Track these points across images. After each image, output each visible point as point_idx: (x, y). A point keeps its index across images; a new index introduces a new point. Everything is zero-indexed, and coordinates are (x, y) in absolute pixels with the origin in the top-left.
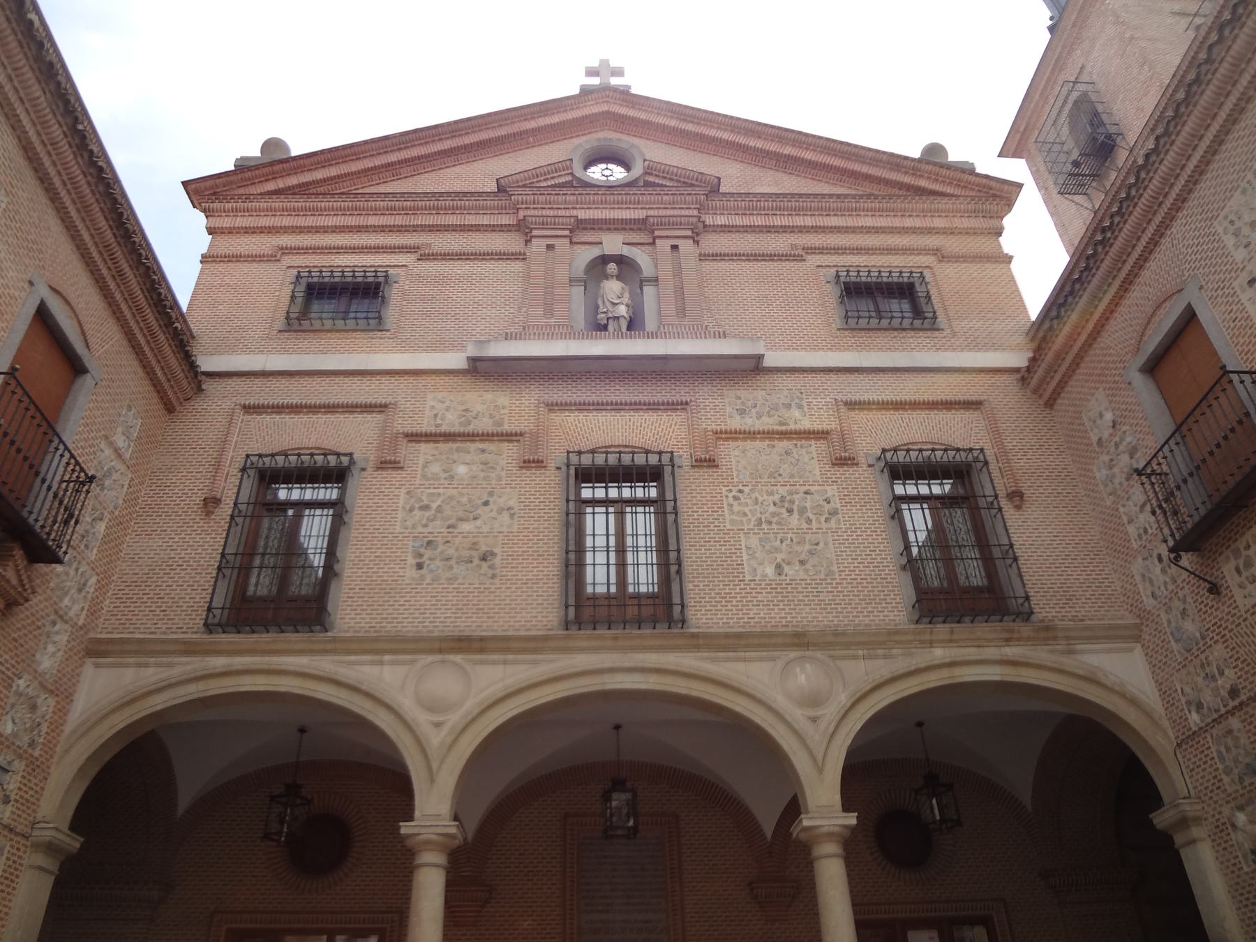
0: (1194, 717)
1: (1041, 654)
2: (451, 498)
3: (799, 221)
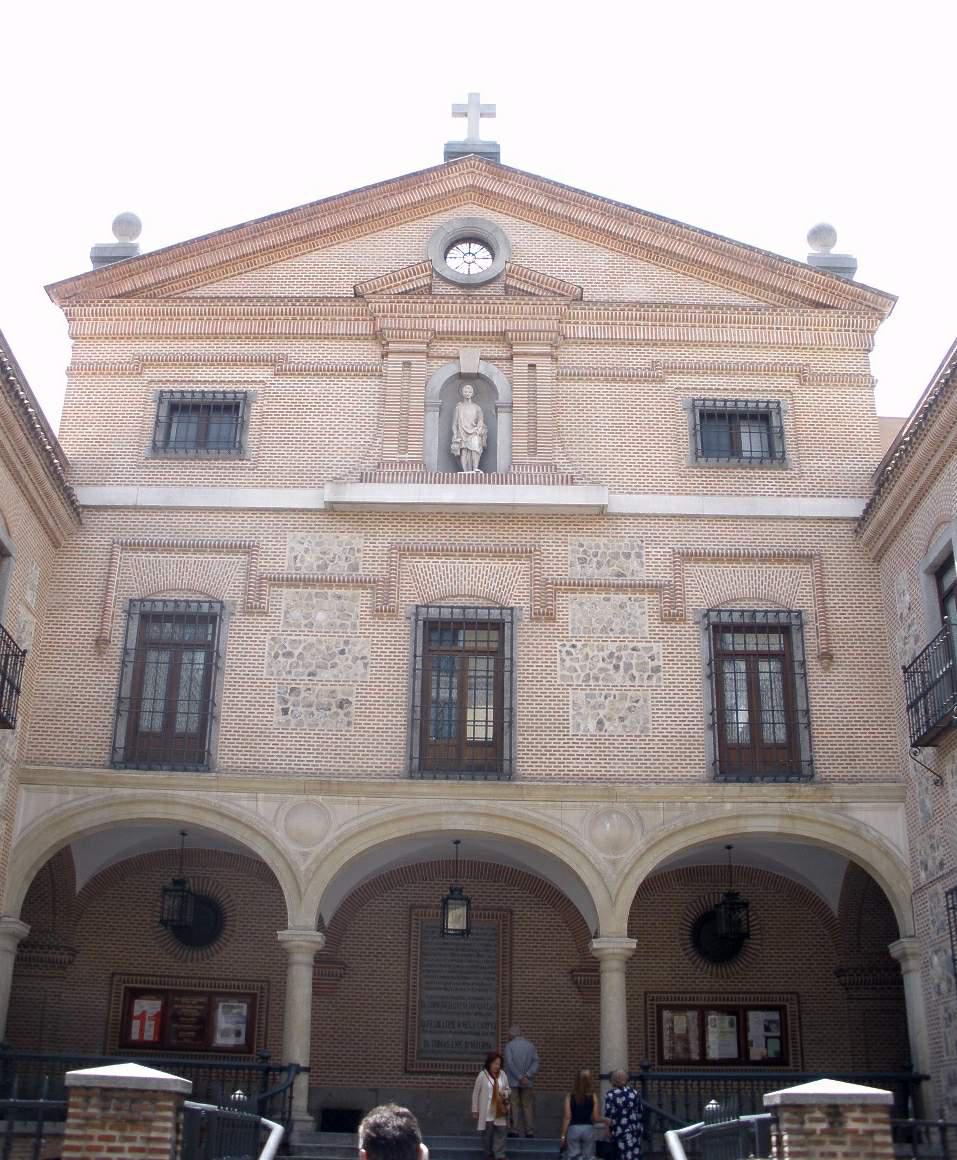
0: (923, 875)
1: (818, 811)
2: (311, 645)
3: (663, 333)
